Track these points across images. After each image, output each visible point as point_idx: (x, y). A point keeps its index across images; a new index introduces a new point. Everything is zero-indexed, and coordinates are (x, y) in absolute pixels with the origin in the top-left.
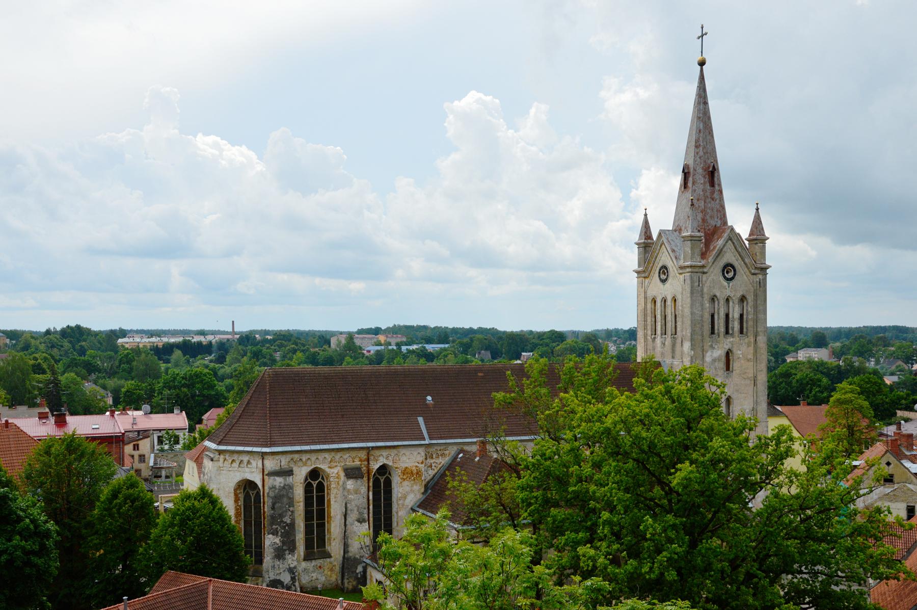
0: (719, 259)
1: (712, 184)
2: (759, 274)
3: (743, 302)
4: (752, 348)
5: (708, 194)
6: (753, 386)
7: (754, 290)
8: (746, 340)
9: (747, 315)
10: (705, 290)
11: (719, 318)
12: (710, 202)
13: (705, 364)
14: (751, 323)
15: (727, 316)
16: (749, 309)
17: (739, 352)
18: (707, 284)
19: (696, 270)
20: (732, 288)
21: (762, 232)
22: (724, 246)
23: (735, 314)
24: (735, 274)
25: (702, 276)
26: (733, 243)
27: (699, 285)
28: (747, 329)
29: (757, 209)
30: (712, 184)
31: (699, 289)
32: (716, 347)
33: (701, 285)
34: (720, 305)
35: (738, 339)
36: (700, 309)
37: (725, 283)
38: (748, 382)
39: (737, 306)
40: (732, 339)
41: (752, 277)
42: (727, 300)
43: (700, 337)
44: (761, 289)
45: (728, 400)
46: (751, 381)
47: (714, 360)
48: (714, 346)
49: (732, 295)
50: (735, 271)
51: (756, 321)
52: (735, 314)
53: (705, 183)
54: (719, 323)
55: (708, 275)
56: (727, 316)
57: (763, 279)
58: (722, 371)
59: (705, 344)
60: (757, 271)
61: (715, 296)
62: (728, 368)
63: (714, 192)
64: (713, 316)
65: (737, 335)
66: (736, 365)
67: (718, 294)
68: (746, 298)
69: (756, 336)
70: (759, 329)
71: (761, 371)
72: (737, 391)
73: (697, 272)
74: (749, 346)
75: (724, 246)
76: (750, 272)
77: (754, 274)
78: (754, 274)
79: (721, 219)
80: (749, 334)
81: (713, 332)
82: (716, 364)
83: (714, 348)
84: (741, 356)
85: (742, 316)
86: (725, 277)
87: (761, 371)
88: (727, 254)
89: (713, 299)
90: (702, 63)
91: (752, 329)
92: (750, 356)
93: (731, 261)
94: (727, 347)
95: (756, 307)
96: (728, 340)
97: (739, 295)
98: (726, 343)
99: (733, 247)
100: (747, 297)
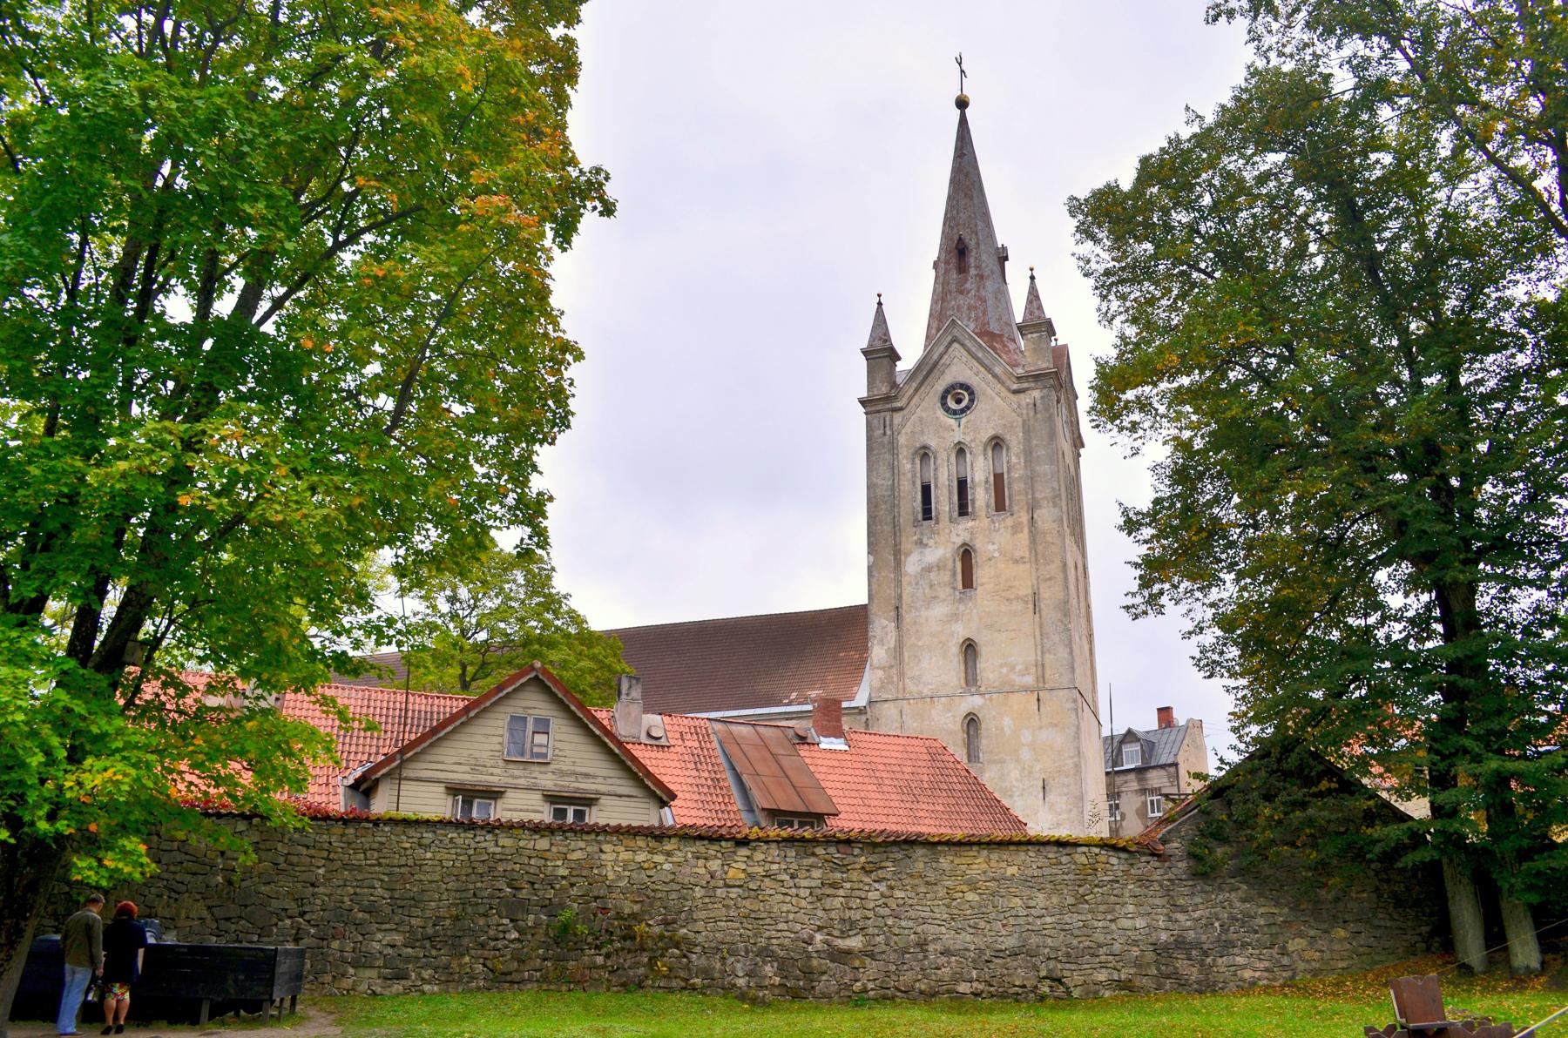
0: (930, 379)
1: (962, 268)
2: (1028, 389)
3: (1001, 447)
4: (1024, 536)
5: (953, 287)
6: (1032, 611)
7: (1024, 421)
8: (1010, 521)
9: (1009, 473)
10: (902, 439)
11: (936, 486)
12: (955, 299)
13: (905, 580)
14: (1018, 486)
15: (962, 485)
16: (1014, 460)
17: (991, 547)
18: (908, 428)
19: (880, 407)
20: (966, 427)
21: (1037, 313)
22: (941, 357)
23: (980, 471)
24: (972, 401)
25: (892, 417)
26: (963, 345)
27: (885, 434)
28: (1010, 496)
29: (1032, 278)
30: (962, 268)
31: (886, 439)
32: (931, 542)
33: (889, 432)
34: (939, 461)
35: (986, 521)
36: (888, 475)
37: (951, 421)
38: (1020, 606)
39: (981, 458)
40: (970, 524)
41: (1014, 398)
42: (961, 451)
43: (888, 528)
44: (1039, 416)
45: (970, 649)
46: (1027, 602)
47: (928, 569)
48: (925, 541)
49: (967, 439)
50: (971, 393)
51: (1031, 480)
52: (980, 471)
53: (947, 271)
54: (937, 497)
55: (905, 412)
56: (962, 485)
57: (1042, 398)
58: (948, 590)
59: (903, 539)
60: (1025, 385)
61: (925, 447)
62: (968, 582)
63: (966, 280)
64: (926, 490)
65: (983, 513)
66: (981, 574)
67: (933, 443)
68: (1003, 440)
69: (1032, 509)
70: (1038, 496)
71: (1050, 579)
72: (990, 626)
73: (879, 412)
74: (1016, 529)
75: (941, 357)
76: (1009, 389)
77: (1016, 392)
78: (1016, 392)
79: (976, 320)
80: (1015, 508)
81: (927, 513)
82: (933, 576)
83: (926, 546)
84: (996, 554)
85: (999, 478)
86: (947, 410)
87: (1050, 579)
88: (953, 368)
89: (924, 454)
90: (962, 104)
91: (1022, 497)
92: (1023, 551)
93: (961, 379)
94: (959, 541)
95: (1028, 452)
96: (961, 527)
97: (985, 435)
98: (961, 532)
99: (965, 353)
100: (1007, 437)
